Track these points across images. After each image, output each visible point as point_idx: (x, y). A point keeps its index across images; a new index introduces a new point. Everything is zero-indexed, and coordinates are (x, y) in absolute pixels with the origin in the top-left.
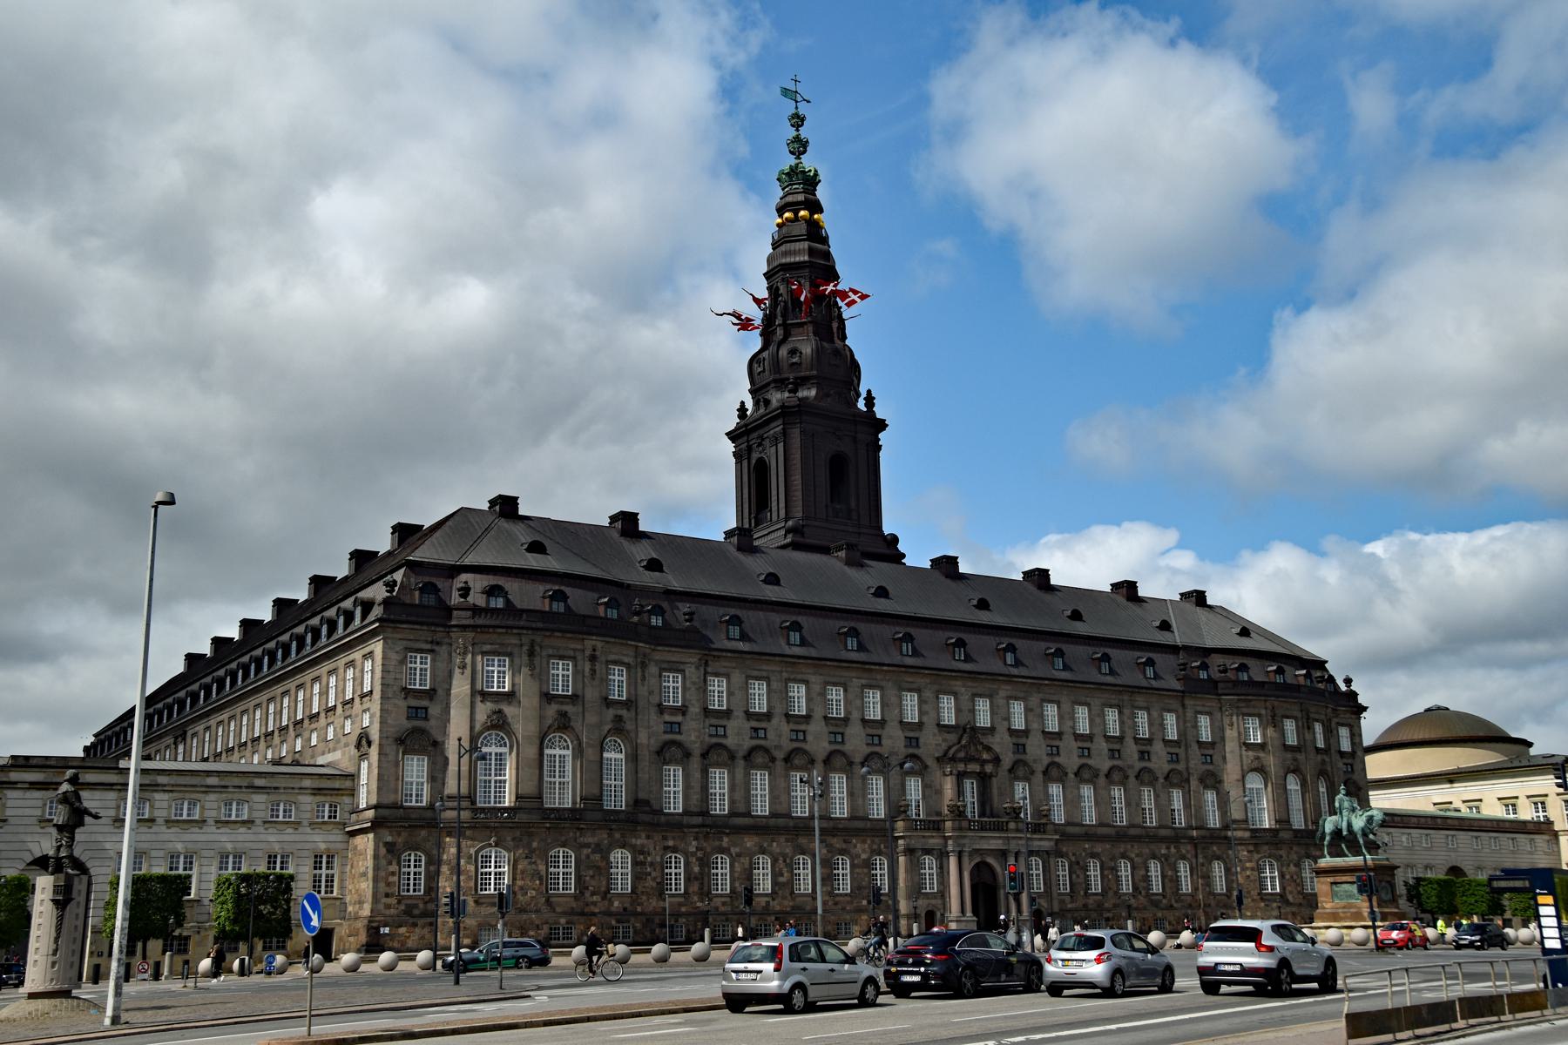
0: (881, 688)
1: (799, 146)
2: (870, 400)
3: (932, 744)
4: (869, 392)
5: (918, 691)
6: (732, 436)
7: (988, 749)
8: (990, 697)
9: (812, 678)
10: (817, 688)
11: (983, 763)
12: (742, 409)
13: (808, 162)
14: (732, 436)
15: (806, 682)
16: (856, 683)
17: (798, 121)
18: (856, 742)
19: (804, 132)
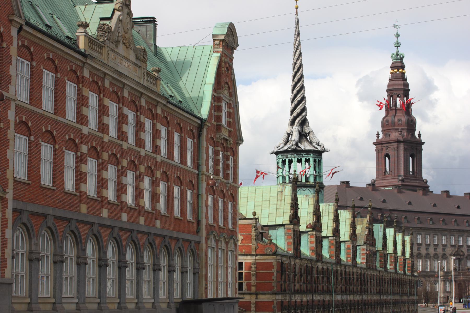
0: (437, 235)
1: (398, 45)
2: (420, 135)
3: (449, 250)
4: (419, 132)
5: (446, 235)
6: (375, 144)
7: (462, 251)
8: (462, 236)
9: (423, 233)
10: (423, 236)
11: (460, 255)
12: (378, 135)
13: (401, 50)
14: (375, 144)
15: (421, 234)
16: (432, 234)
17: (397, 36)
18: (431, 251)
19: (400, 40)
